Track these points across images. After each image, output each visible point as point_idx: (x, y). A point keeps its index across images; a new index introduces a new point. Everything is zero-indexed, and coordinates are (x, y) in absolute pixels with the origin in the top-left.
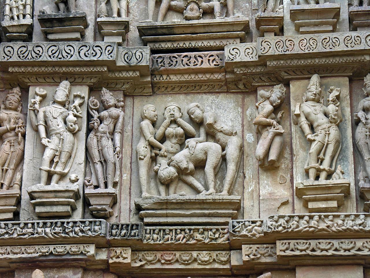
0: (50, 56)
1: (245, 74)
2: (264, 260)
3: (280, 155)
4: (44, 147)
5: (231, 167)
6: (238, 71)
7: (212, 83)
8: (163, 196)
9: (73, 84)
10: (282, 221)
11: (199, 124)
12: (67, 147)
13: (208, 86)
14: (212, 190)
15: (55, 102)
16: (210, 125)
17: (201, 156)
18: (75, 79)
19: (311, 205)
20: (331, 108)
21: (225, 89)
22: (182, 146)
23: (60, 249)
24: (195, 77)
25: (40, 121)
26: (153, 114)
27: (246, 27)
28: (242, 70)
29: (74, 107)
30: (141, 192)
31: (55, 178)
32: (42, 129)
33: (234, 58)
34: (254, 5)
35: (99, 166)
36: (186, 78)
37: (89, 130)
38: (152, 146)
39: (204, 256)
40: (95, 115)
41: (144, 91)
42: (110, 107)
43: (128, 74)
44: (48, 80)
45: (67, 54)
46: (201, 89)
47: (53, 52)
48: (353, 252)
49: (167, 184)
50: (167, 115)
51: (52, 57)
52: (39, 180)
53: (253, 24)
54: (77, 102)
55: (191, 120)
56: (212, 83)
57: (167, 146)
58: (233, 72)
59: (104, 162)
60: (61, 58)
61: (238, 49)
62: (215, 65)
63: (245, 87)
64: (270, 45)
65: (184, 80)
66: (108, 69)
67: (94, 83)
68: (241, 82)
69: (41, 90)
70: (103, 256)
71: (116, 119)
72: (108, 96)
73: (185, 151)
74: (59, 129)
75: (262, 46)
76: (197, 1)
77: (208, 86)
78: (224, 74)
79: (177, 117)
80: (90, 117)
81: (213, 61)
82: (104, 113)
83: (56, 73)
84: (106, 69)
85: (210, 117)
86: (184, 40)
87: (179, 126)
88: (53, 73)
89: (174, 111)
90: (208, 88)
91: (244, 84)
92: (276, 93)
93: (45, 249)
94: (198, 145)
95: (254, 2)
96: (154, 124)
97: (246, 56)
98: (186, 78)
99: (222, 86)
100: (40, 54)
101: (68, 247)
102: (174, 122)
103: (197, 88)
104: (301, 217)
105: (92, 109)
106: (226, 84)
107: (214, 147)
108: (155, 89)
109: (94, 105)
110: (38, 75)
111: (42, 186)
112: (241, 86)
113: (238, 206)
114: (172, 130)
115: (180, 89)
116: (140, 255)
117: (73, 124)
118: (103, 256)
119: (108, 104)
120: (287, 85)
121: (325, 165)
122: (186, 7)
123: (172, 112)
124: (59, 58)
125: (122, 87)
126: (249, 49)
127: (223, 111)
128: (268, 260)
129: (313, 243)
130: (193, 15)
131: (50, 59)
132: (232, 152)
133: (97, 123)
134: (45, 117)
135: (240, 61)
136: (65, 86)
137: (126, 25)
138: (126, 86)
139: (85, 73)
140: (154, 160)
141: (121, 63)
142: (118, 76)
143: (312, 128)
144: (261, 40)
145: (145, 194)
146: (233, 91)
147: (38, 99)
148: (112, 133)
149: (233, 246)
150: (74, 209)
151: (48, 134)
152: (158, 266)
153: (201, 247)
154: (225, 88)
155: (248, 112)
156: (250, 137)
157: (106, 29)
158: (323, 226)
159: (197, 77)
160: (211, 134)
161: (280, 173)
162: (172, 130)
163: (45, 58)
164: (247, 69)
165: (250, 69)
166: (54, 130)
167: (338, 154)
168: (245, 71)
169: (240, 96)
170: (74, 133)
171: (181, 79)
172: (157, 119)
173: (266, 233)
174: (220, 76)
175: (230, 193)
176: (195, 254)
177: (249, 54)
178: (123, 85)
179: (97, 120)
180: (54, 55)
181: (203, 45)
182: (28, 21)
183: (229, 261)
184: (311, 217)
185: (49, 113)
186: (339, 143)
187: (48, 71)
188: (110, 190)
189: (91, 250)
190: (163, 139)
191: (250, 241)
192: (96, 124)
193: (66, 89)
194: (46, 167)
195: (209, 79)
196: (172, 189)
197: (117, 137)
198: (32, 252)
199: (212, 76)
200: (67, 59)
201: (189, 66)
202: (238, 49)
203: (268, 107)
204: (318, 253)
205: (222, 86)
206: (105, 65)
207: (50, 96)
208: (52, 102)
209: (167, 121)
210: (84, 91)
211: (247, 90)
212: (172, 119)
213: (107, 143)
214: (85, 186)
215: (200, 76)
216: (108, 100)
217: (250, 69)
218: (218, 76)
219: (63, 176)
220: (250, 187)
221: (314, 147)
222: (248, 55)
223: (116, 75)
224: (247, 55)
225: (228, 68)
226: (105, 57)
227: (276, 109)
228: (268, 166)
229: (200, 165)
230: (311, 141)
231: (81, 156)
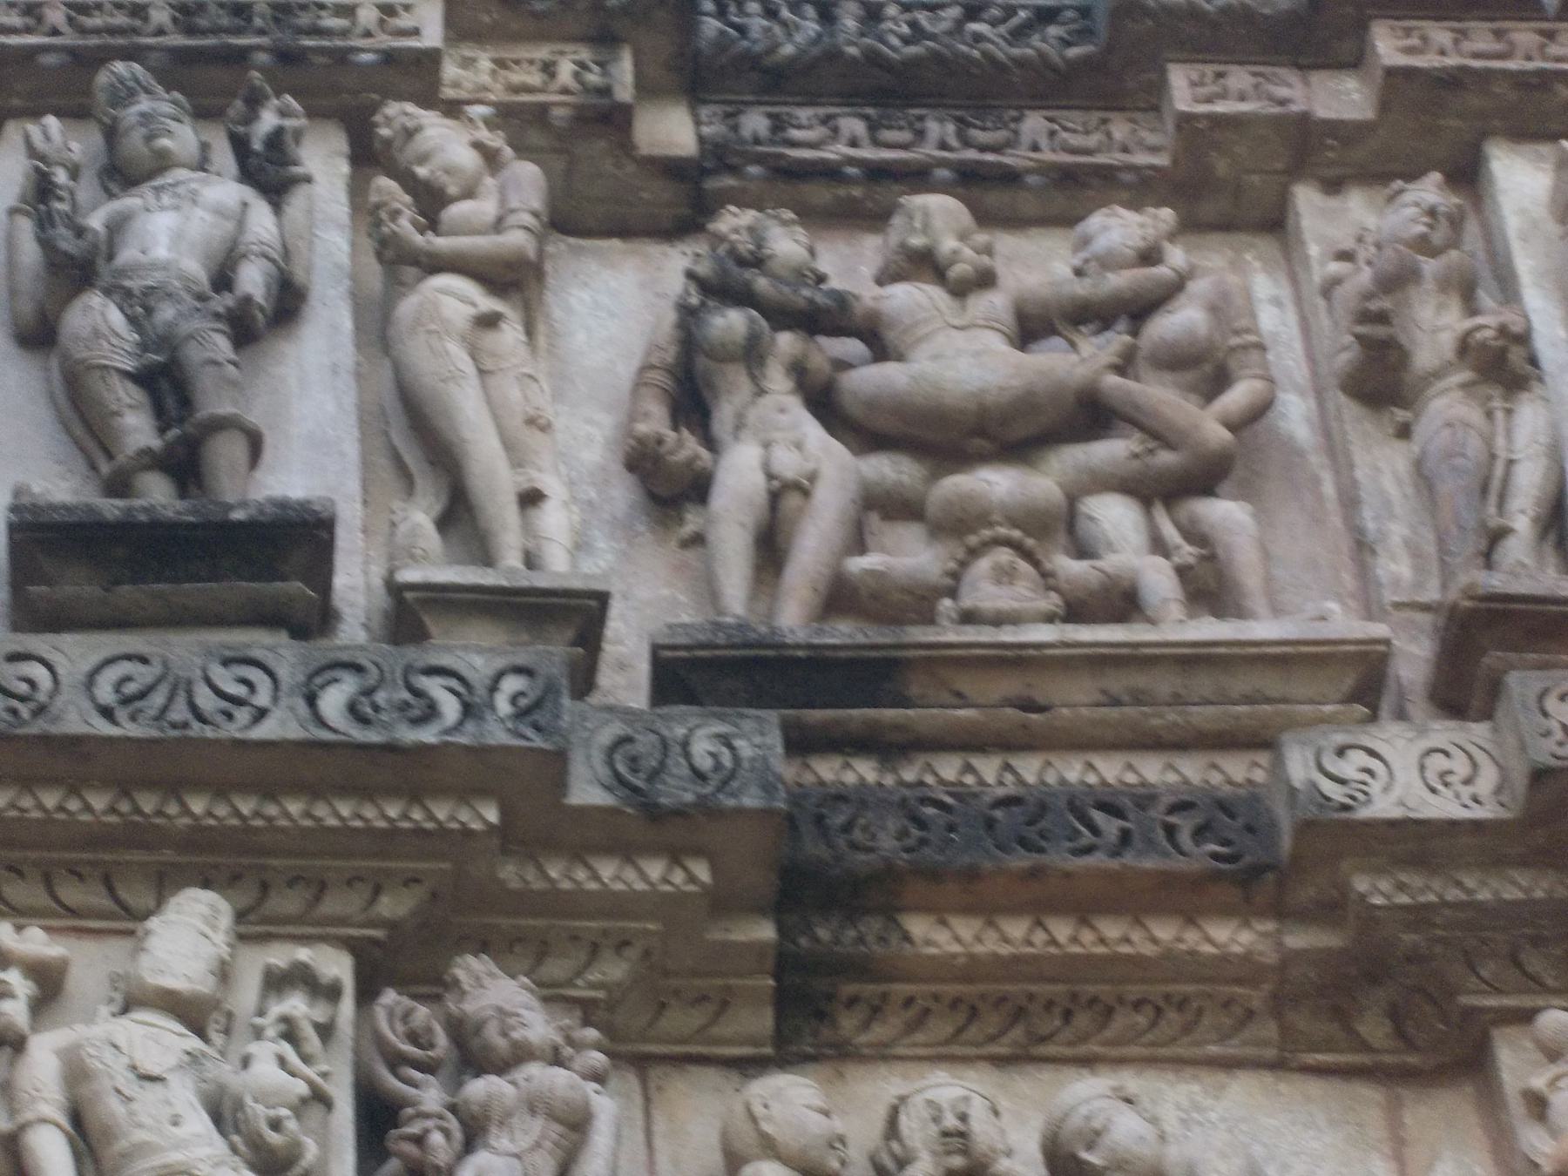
0: (107, 713)
1: (1419, 916)
6: (1375, 888)
7: (1190, 988)
9: (252, 927)
13: (1159, 1011)
18: (264, 882)
21: (1265, 1043)
24: (1074, 940)
25: (34, 1100)
26: (817, 1125)
28: (1401, 887)
29: (282, 1027)
33: (1353, 798)
34: (1396, 582)
40: (431, 1096)
41: (724, 1029)
42: (522, 1054)
43: (630, 874)
44: (72, 894)
45: (224, 704)
46: (1108, 1034)
47: (131, 688)
51: (122, 714)
56: (1190, 988)
58: (1333, 908)
60: (185, 725)
61: (1372, 753)
62: (1215, 856)
63: (1400, 1033)
65: (1005, 950)
66: (504, 813)
67: (392, 925)
71: (577, 1124)
74: (179, 1145)
75: (1545, 714)
76: (1030, 542)
77: (1159, 1011)
78: (1269, 926)
79: (994, 1151)
81: (1200, 833)
83: (138, 835)
84: (492, 815)
85: (1223, 1156)
86: (969, 743)
89: (963, 1118)
90: (1153, 1024)
91: (1395, 1015)
95: (1393, 567)
97: (1433, 791)
99: (1250, 1014)
100: (42, 697)
103: (1082, 1020)
105: (396, 1061)
106: (1279, 1005)
109: (413, 1037)
112: (1375, 1028)
115: (960, 1030)
117: (284, 1112)
119: (515, 1035)
122: (956, 576)
123: (951, 1122)
124: (174, 726)
125: (579, 974)
126: (1447, 754)
130: (1016, 605)
131: (104, 728)
133: (447, 1133)
134: (76, 1073)
135: (1397, 813)
136: (205, 910)
138: (614, 970)
139: (343, 840)
142: (566, 885)
144: (1537, 687)
146: (1320, 1057)
154: (1270, 1030)
159: (1087, 936)
164: (1436, 884)
165: (1459, 884)
166: (142, 1149)
168: (1422, 891)
169: (1369, 1095)
171: (979, 949)
172: (843, 1163)
174: (1246, 937)
177: (1449, 779)
178: (588, 965)
179: (441, 1117)
180: (138, 704)
181: (1092, 779)
185: (108, 1054)
187: (86, 817)
192: (437, 1138)
193: (214, 928)
195: (1168, 955)
199: (1191, 937)
200: (232, 731)
201: (1041, 850)
202: (1372, 753)
205: (1250, 1014)
206: (484, 792)
208: (115, 1008)
211: (1412, 1059)
212: (957, 1161)
215: (1112, 929)
216: (508, 1007)
217: (1459, 884)
222: (1446, 785)
223: (553, 874)
224: (1440, 787)
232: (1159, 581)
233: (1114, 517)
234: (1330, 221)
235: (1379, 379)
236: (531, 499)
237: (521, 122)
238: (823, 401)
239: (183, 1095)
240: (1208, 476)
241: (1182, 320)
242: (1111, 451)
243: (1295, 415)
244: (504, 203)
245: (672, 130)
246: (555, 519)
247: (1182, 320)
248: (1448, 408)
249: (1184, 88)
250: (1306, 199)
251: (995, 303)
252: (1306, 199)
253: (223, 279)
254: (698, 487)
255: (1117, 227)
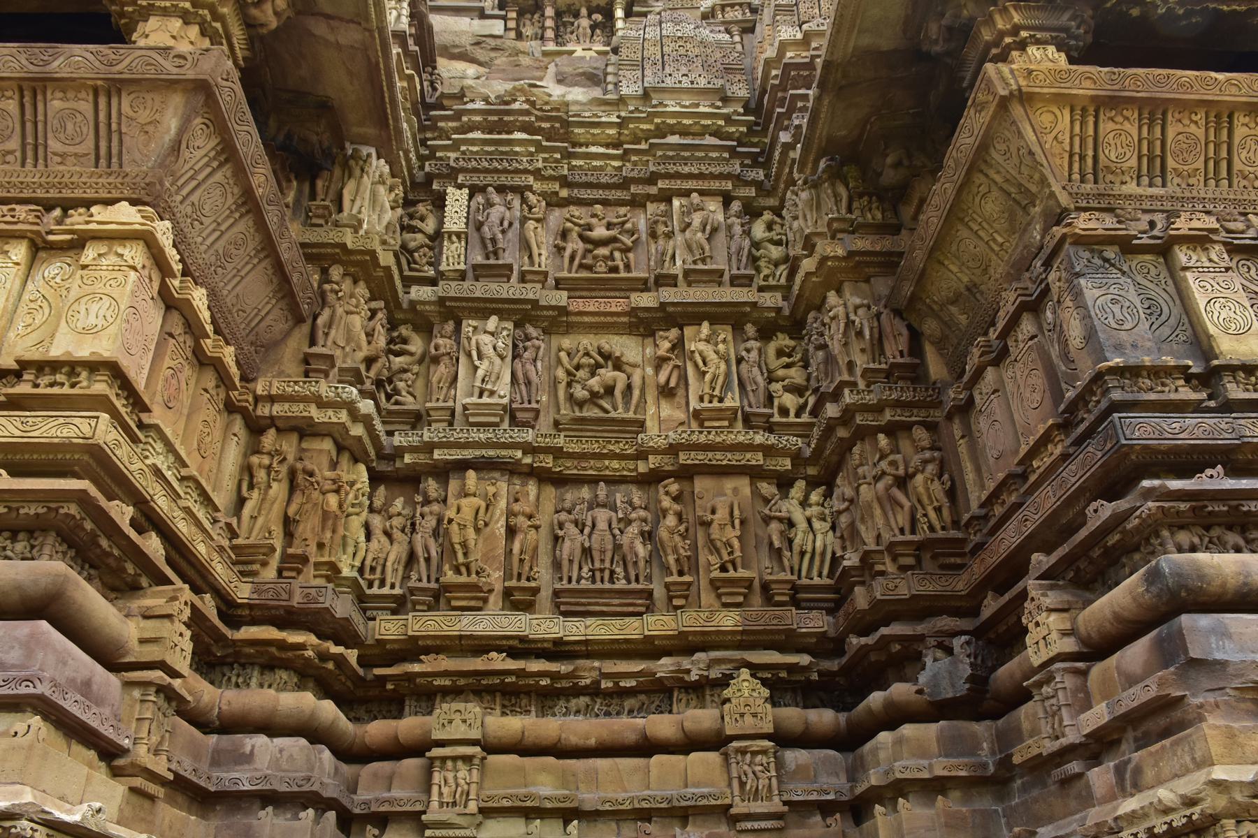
2: (667, 468)
3: (678, 384)
4: (476, 368)
5: (636, 393)
8: (578, 414)
9: (501, 319)
10: (684, 435)
11: (607, 356)
12: (496, 369)
14: (620, 410)
15: (485, 332)
16: (618, 358)
17: (611, 383)
18: (503, 315)
19: (707, 424)
20: (721, 347)
22: (593, 374)
23: (491, 453)
27: (645, 281)
30: (559, 410)
31: (486, 394)
32: (474, 353)
35: (523, 387)
36: (596, 319)
37: (514, 358)
38: (569, 373)
39: (615, 464)
48: (743, 462)
49: (581, 404)
50: (581, 348)
52: (472, 395)
53: (652, 280)
54: (505, 333)
55: (600, 353)
57: (581, 374)
59: (528, 383)
64: (668, 295)
68: (644, 325)
69: (474, 323)
70: (528, 460)
71: (538, 348)
72: (531, 330)
73: (597, 378)
80: (515, 346)
82: (528, 343)
87: (591, 357)
88: (484, 308)
92: (674, 333)
93: (478, 453)
94: (608, 374)
96: (569, 354)
98: (596, 319)
101: (498, 451)
102: (587, 354)
104: (701, 432)
107: (621, 377)
108: (569, 329)
110: (471, 310)
111: (475, 400)
113: (642, 424)
114: (585, 360)
116: (560, 462)
118: (528, 460)
120: (682, 329)
121: (717, 392)
127: (629, 348)
128: (670, 468)
129: (710, 455)
132: (636, 380)
134: (477, 343)
137: (546, 274)
138: (546, 324)
140: (569, 385)
141: (543, 303)
143: (705, 364)
145: (563, 412)
147: (471, 329)
148: (535, 360)
149: (642, 455)
150: (502, 421)
151: (480, 357)
152: (575, 472)
153: (613, 456)
155: (648, 351)
156: (650, 371)
157: (529, 277)
158: (718, 439)
160: (618, 366)
161: (677, 399)
162: (585, 360)
163: (478, 294)
167: (727, 386)
170: (502, 358)
173: (671, 445)
175: (635, 413)
176: (607, 462)
182: (462, 267)
183: (636, 469)
184: (709, 433)
186: (728, 375)
188: (534, 405)
189: (519, 454)
190: (578, 367)
191: (656, 451)
194: (478, 383)
196: (585, 409)
197: (539, 364)
198: (468, 454)
203: (667, 345)
204: (714, 462)
207: (480, 327)
209: (581, 353)
210: (510, 325)
213: (530, 367)
214: (511, 401)
218: (625, 319)
219: (492, 393)
220: (651, 410)
221: (708, 377)
225: (634, 311)
226: (531, 296)
227: (673, 348)
228: (666, 392)
229: (610, 390)
230: (704, 373)
231: (507, 377)
232: (621, 267)
233: (617, 255)
234: (651, 207)
235: (653, 235)
236: (540, 255)
237: (543, 195)
238: (581, 236)
239: (490, 347)
240: (628, 250)
241: (628, 226)
242: (618, 245)
243: (644, 237)
244: (540, 209)
245: (564, 193)
246: (543, 258)
247: (628, 226)
248: (661, 242)
249: (633, 189)
250: (648, 204)
251: (604, 222)
252: (648, 204)
253: (501, 224)
254: (564, 249)
255: (623, 210)
